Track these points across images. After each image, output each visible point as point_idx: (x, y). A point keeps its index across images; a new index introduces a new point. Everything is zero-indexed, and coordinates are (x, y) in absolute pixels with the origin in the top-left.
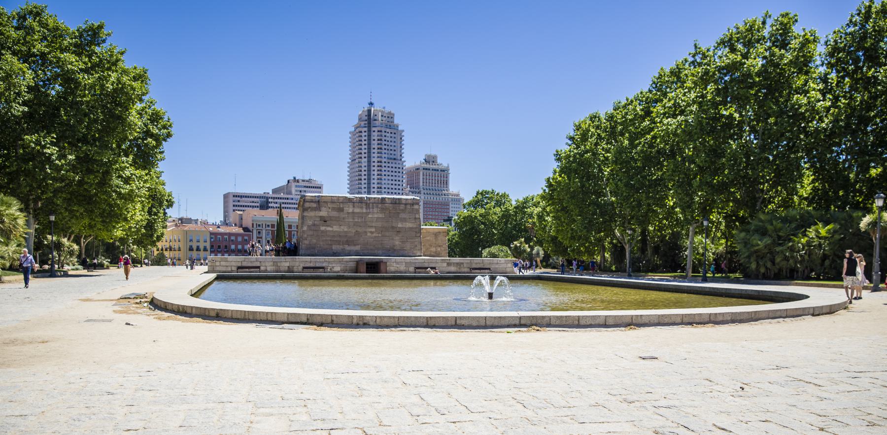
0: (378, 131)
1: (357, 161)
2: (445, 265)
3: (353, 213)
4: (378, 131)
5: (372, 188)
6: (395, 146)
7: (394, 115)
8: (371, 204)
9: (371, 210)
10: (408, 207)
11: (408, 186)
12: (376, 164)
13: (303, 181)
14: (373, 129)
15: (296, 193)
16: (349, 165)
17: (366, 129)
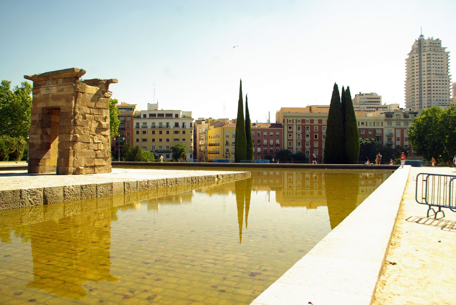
0: (428, 55)
1: (411, 79)
4: (428, 55)
7: (441, 41)
13: (366, 94)
14: (423, 54)
16: (405, 83)
17: (417, 55)
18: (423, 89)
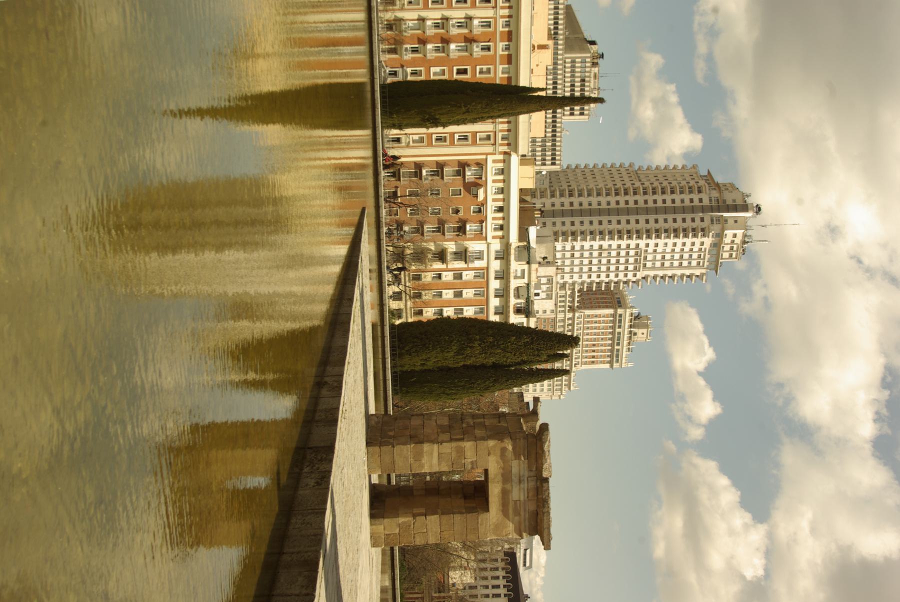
1: (637, 184)
5: (581, 219)
16: (627, 165)
17: (706, 202)
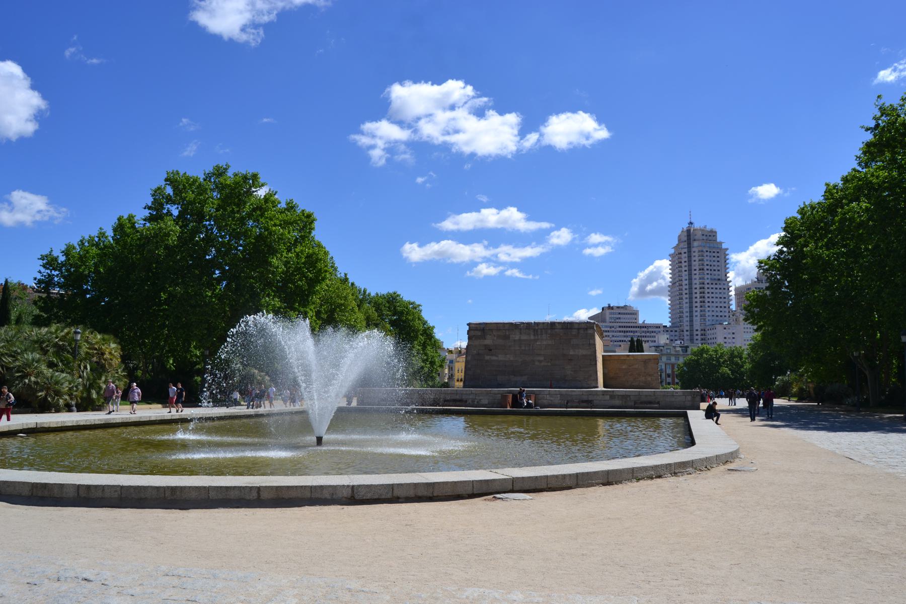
1: (677, 284)
2: (608, 397)
3: (520, 340)
5: (694, 312)
6: (718, 266)
7: (716, 232)
8: (539, 331)
9: (539, 336)
10: (582, 332)
11: (739, 308)
12: (698, 286)
13: (618, 307)
15: (610, 320)
18: (694, 300)
